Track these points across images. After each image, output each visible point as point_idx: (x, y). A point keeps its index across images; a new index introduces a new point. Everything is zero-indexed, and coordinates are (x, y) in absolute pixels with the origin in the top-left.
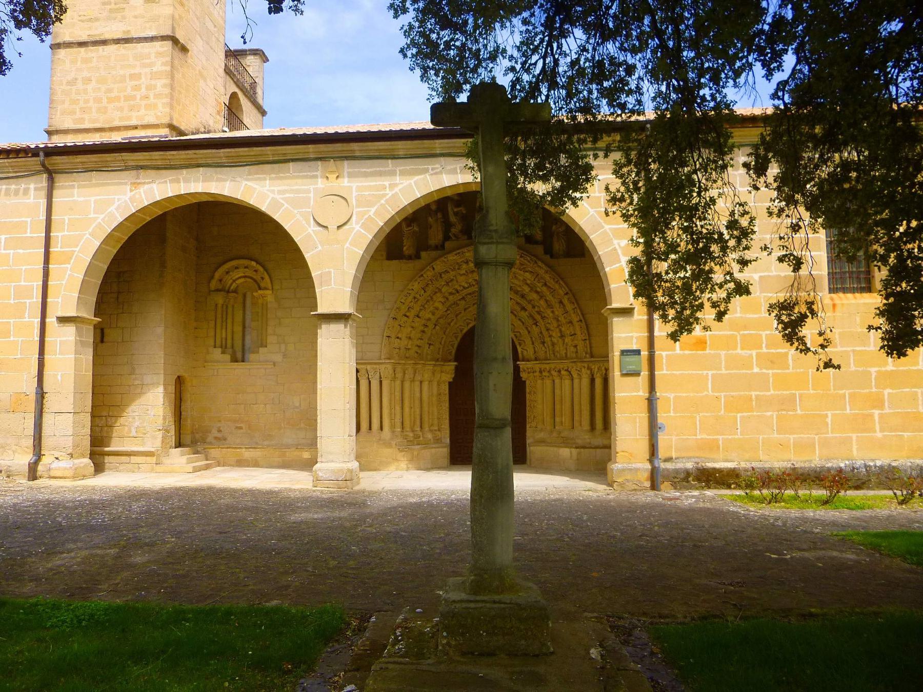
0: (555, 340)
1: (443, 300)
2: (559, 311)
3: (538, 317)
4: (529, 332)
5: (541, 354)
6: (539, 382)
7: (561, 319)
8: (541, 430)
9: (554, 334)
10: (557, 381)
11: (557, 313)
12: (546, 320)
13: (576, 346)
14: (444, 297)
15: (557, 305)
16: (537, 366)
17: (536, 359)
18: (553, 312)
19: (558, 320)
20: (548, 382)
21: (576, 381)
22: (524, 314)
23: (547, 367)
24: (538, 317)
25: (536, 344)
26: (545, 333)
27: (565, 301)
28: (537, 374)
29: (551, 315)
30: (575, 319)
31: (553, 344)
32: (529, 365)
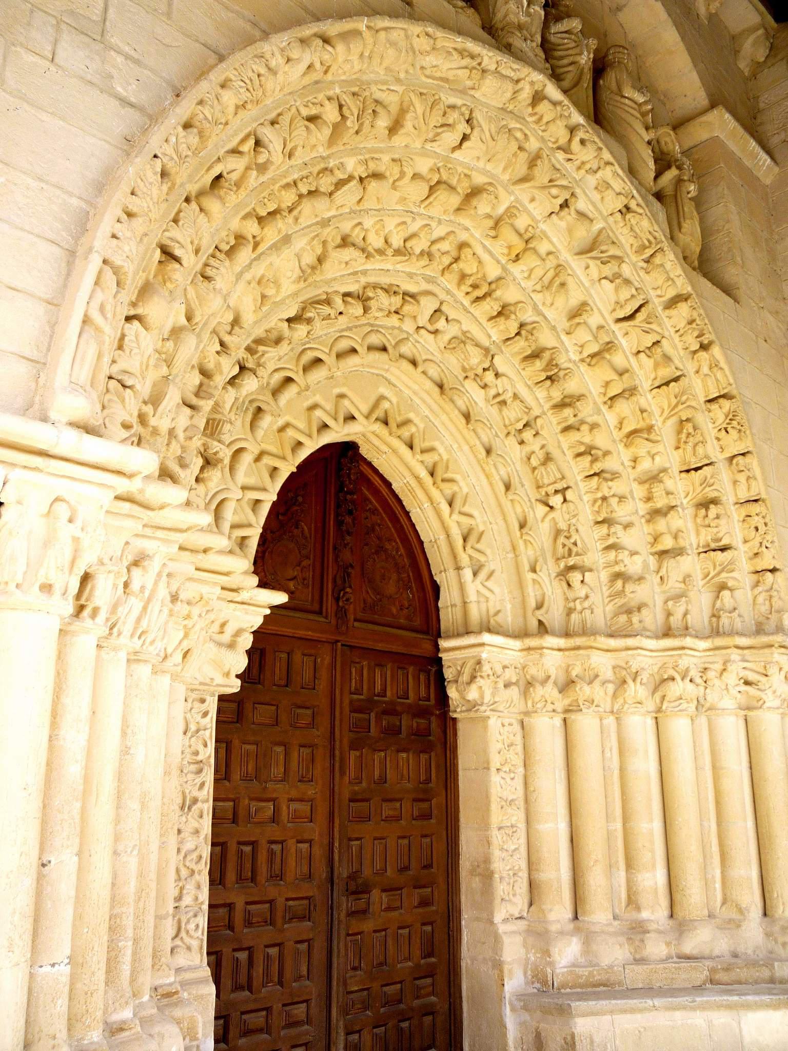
0: (634, 566)
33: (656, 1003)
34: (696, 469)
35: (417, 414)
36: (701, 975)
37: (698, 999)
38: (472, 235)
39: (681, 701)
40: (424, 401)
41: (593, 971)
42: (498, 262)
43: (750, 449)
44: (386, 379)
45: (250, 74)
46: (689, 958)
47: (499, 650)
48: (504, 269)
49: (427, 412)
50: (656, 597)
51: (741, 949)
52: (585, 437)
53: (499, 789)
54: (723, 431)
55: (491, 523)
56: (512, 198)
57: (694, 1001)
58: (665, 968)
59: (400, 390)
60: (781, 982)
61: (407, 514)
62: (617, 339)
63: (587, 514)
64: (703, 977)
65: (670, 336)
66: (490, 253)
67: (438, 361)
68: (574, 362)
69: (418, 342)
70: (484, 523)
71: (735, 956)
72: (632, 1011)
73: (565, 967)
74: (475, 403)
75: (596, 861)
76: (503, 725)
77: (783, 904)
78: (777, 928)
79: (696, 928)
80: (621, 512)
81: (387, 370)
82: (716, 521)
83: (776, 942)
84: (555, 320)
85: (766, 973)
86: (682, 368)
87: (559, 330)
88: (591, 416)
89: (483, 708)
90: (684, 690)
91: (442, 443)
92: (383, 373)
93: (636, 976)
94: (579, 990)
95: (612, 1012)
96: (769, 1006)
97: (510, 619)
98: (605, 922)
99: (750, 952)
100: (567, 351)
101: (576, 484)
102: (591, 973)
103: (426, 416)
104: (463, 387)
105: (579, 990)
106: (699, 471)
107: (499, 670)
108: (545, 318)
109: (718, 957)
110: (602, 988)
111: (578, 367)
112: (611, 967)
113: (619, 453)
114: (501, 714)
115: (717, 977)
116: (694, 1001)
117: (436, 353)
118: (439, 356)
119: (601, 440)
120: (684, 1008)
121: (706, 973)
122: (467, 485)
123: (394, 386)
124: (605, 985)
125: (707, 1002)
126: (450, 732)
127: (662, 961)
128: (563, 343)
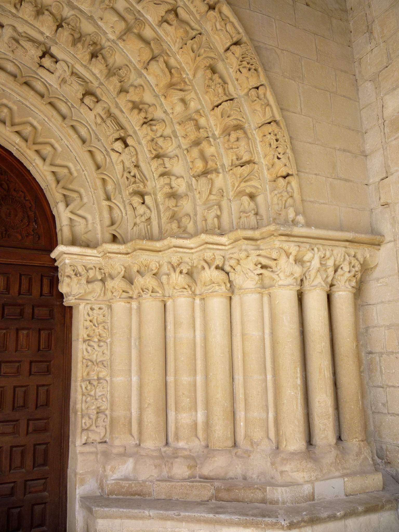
0: (180, 186)
2: (200, 99)
3: (132, 121)
4: (98, 167)
5: (127, 227)
6: (120, 306)
7: (213, 123)
8: (125, 455)
9: (177, 167)
10: (181, 304)
11: (193, 105)
12: (159, 128)
13: (252, 197)
15: (200, 78)
16: (116, 259)
17: (114, 239)
18: (183, 101)
19: (198, 127)
20: (151, 306)
21: (249, 303)
22: (89, 117)
23: (152, 260)
24: (132, 121)
25: (117, 200)
26: (151, 168)
27: (229, 67)
28: (118, 284)
29: (179, 108)
30: (253, 116)
31: (173, 195)
32: (92, 257)
33: (151, 514)
34: (217, 106)
35: (9, 99)
36: (206, 492)
37: (182, 514)
39: (214, 285)
40: (12, 90)
41: (131, 484)
43: (262, 83)
46: (207, 479)
47: (79, 257)
49: (19, 98)
50: (198, 208)
51: (249, 474)
52: (133, 96)
53: (85, 353)
54: (238, 72)
55: (83, 171)
57: (179, 515)
58: (182, 486)
60: (271, 503)
61: (29, 171)
62: (143, 16)
63: (145, 154)
64: (210, 494)
65: (185, 4)
67: (11, 59)
68: (113, 41)
70: (77, 171)
71: (245, 478)
72: (135, 517)
73: (113, 480)
74: (50, 85)
75: (149, 404)
76: (92, 309)
77: (286, 440)
78: (278, 459)
79: (214, 456)
80: (169, 148)
82: (237, 143)
83: (277, 470)
84: (91, 12)
85: (259, 495)
86: (199, 28)
87: (96, 18)
88: (136, 80)
89: (70, 298)
90: (211, 275)
91: (35, 118)
93: (160, 490)
94: (121, 497)
95: (120, 517)
96: (238, 524)
97: (99, 236)
98: (153, 448)
99: (254, 476)
100: (105, 33)
101: (135, 132)
102: (130, 485)
103: (19, 101)
104: (37, 74)
105: (121, 497)
106: (220, 107)
107: (80, 269)
108: (81, 11)
109: (231, 478)
110: (137, 497)
111: (117, 44)
112: (144, 482)
113: (162, 104)
114: (88, 302)
115: (220, 495)
116: (179, 515)
117: (8, 53)
118: (10, 54)
119: (148, 98)
120: (172, 519)
121: (213, 491)
122: (61, 146)
124: (139, 495)
125: (189, 517)
126: (68, 316)
127: (184, 480)
128: (100, 27)
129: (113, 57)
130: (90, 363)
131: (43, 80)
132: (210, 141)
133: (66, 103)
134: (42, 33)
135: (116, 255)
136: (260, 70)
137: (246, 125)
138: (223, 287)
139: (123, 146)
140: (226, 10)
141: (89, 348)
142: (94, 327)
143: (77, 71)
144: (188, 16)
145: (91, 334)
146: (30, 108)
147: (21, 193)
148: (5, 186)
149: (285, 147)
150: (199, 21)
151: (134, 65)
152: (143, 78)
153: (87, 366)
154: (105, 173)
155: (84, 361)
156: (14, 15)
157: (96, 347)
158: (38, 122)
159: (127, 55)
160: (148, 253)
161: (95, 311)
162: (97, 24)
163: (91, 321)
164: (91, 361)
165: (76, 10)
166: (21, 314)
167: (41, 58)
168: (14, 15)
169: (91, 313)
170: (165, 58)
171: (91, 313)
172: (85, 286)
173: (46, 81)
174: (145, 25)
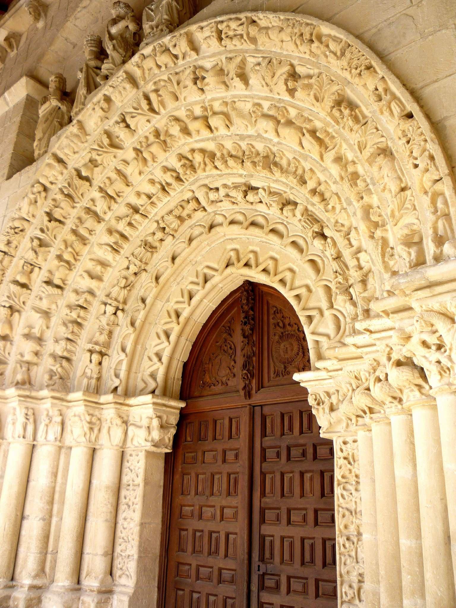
1: (111, 240)
14: (110, 232)
38: (189, 144)
42: (208, 139)
44: (230, 239)
45: (7, 230)
47: (317, 382)
48: (214, 139)
56: (183, 108)
59: (241, 238)
66: (202, 140)
67: (238, 211)
69: (223, 210)
76: (345, 443)
81: (225, 236)
92: (225, 238)
104: (257, 211)
107: (323, 397)
108: (249, 136)
123: (235, 239)
129: (284, 157)
130: (347, 513)
131: (262, 214)
132: (370, 189)
133: (282, 223)
134: (241, 176)
135: (336, 373)
136: (374, 64)
137: (390, 144)
138: (417, 393)
139: (323, 242)
140: (326, 29)
141: (345, 493)
142: (349, 466)
143: (274, 190)
144: (305, 68)
145: (347, 473)
146: (269, 243)
147: (295, 326)
148: (281, 324)
149: (422, 143)
150: (317, 63)
151: (299, 152)
152: (309, 159)
153: (344, 516)
154: (324, 278)
155: (340, 509)
156: (220, 176)
157: (353, 492)
158: (276, 253)
159: (292, 148)
160: (349, 362)
161: (348, 445)
162: (264, 138)
163: (345, 458)
164: (348, 509)
165: (247, 139)
166: (304, 454)
167: (245, 197)
168: (220, 176)
169: (344, 447)
170: (308, 126)
171: (344, 447)
172: (328, 416)
173: (264, 213)
174: (286, 109)
